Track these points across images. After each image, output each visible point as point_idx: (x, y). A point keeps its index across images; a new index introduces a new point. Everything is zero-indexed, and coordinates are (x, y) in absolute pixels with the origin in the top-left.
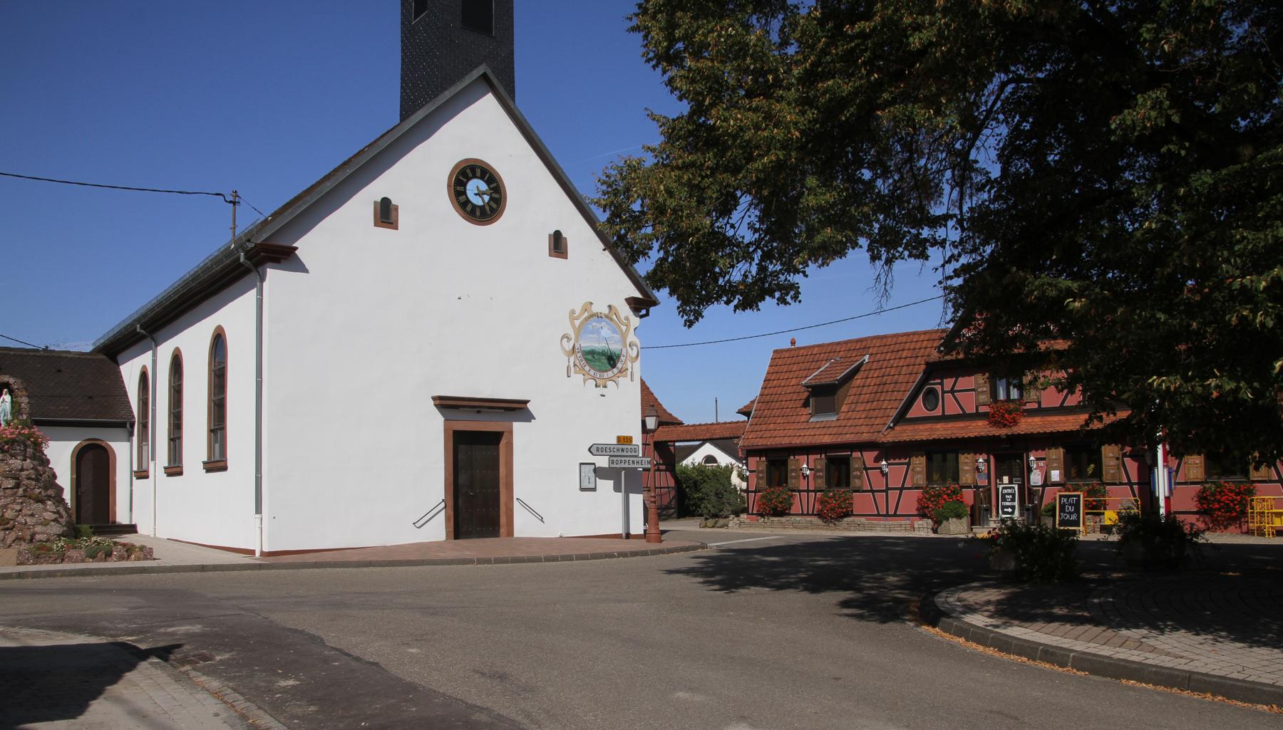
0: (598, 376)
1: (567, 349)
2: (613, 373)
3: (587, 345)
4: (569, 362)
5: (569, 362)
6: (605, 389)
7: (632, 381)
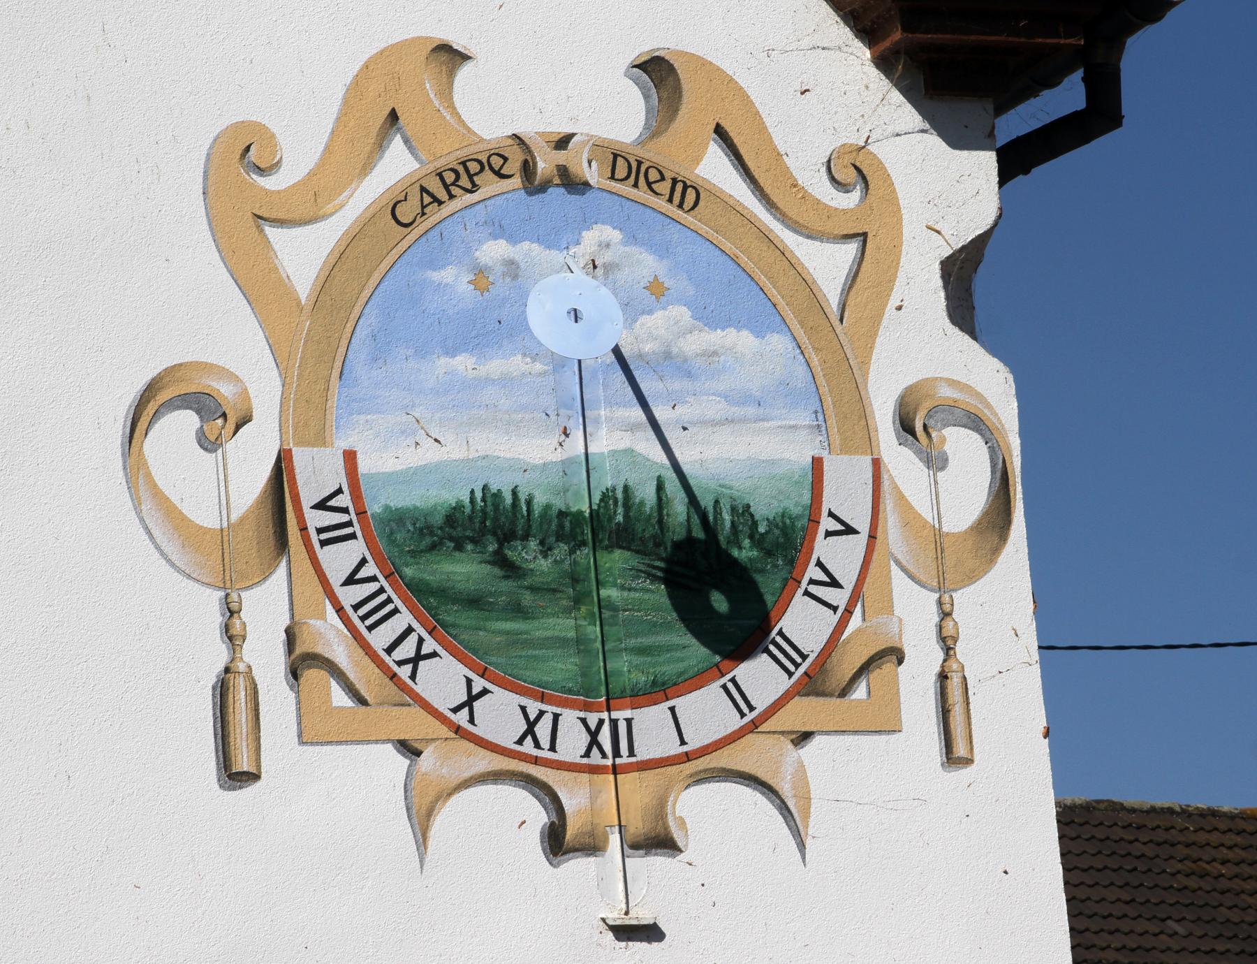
0: (572, 743)
1: (207, 516)
2: (738, 697)
3: (428, 454)
4: (232, 637)
5: (232, 637)
6: (658, 862)
7: (952, 758)
